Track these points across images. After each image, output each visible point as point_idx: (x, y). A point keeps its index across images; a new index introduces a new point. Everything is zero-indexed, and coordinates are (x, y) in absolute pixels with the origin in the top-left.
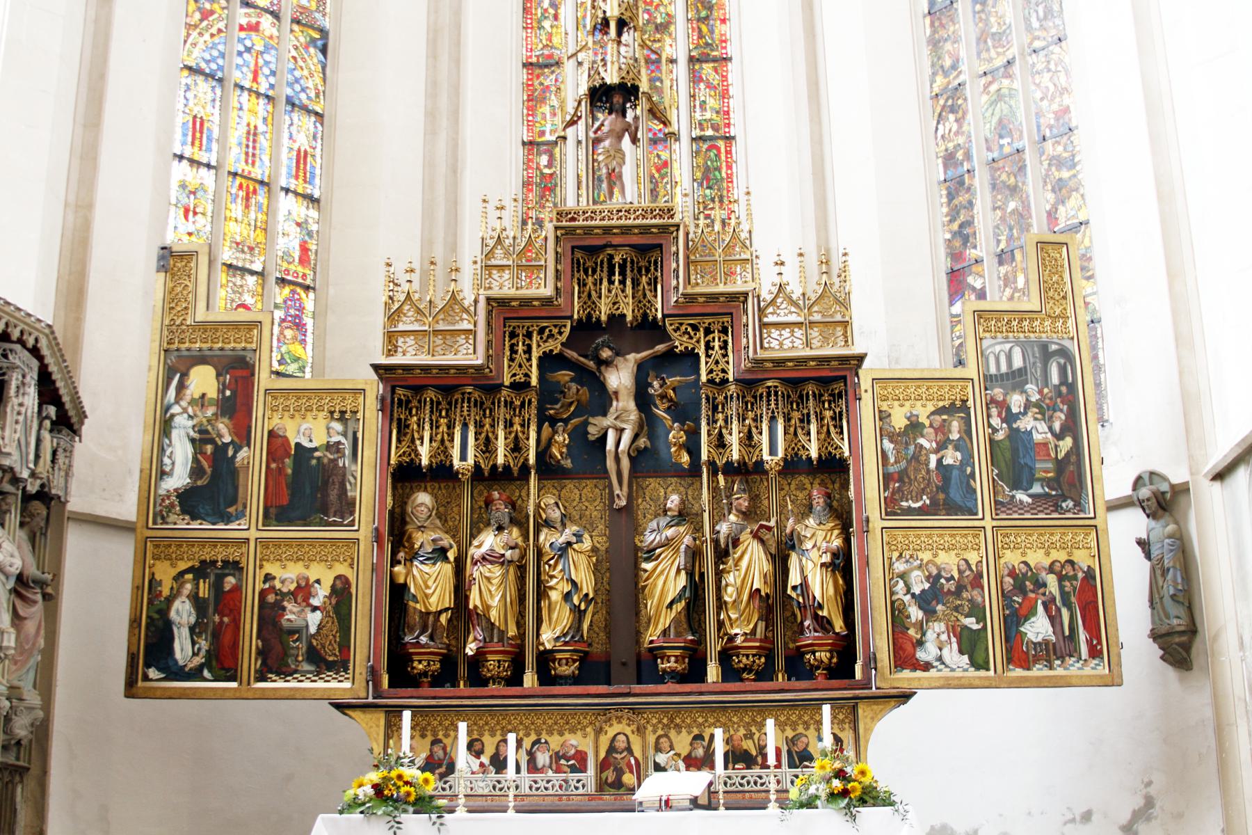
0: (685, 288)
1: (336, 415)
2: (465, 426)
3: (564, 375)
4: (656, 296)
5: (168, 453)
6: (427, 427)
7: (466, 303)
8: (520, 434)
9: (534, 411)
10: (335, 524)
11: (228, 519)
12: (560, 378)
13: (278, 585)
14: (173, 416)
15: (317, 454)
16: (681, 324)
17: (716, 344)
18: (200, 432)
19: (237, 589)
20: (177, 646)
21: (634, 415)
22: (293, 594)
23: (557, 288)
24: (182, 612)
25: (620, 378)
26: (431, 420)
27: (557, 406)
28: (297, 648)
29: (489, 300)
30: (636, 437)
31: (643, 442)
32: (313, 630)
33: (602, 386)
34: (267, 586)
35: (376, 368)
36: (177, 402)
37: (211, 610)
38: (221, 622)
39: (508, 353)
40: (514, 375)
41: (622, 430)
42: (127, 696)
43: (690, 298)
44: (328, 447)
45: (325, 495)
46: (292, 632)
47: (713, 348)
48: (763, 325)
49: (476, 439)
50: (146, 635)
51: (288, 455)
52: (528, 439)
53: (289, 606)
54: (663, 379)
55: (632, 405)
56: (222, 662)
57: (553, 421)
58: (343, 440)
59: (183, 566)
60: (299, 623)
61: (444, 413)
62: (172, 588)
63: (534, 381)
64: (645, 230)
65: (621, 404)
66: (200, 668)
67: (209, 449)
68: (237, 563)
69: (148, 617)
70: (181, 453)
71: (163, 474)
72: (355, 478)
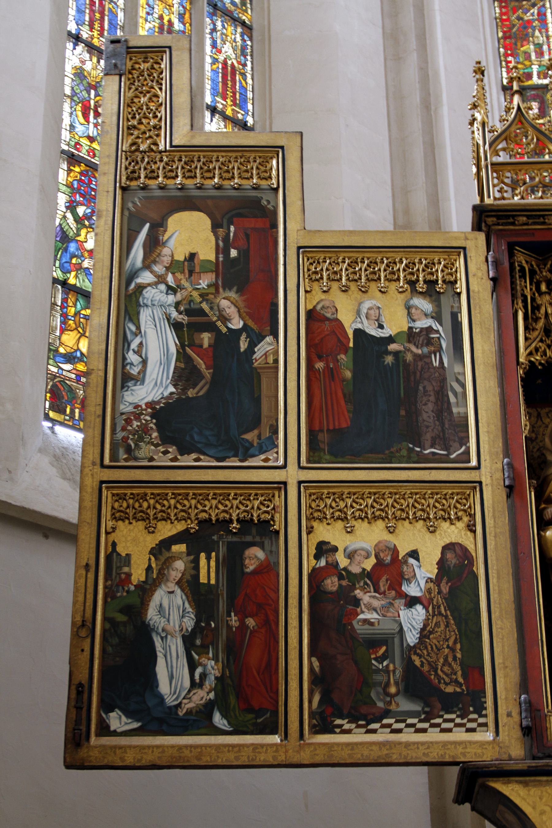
5: (134, 345)
10: (434, 458)
11: (245, 452)
13: (343, 562)
14: (141, 288)
15: (393, 347)
18: (189, 312)
19: (268, 569)
20: (161, 670)
22: (371, 577)
24: (169, 610)
28: (386, 670)
32: (412, 638)
34: (323, 563)
36: (147, 266)
37: (222, 605)
38: (243, 626)
42: (69, 766)
44: (411, 335)
45: (413, 413)
46: (373, 643)
50: (103, 651)
51: (346, 350)
53: (366, 597)
56: (247, 698)
58: (436, 326)
59: (167, 530)
60: (388, 627)
62: (149, 569)
66: (207, 710)
67: (206, 338)
68: (267, 522)
69: (105, 619)
70: (157, 345)
71: (126, 379)
72: (463, 386)
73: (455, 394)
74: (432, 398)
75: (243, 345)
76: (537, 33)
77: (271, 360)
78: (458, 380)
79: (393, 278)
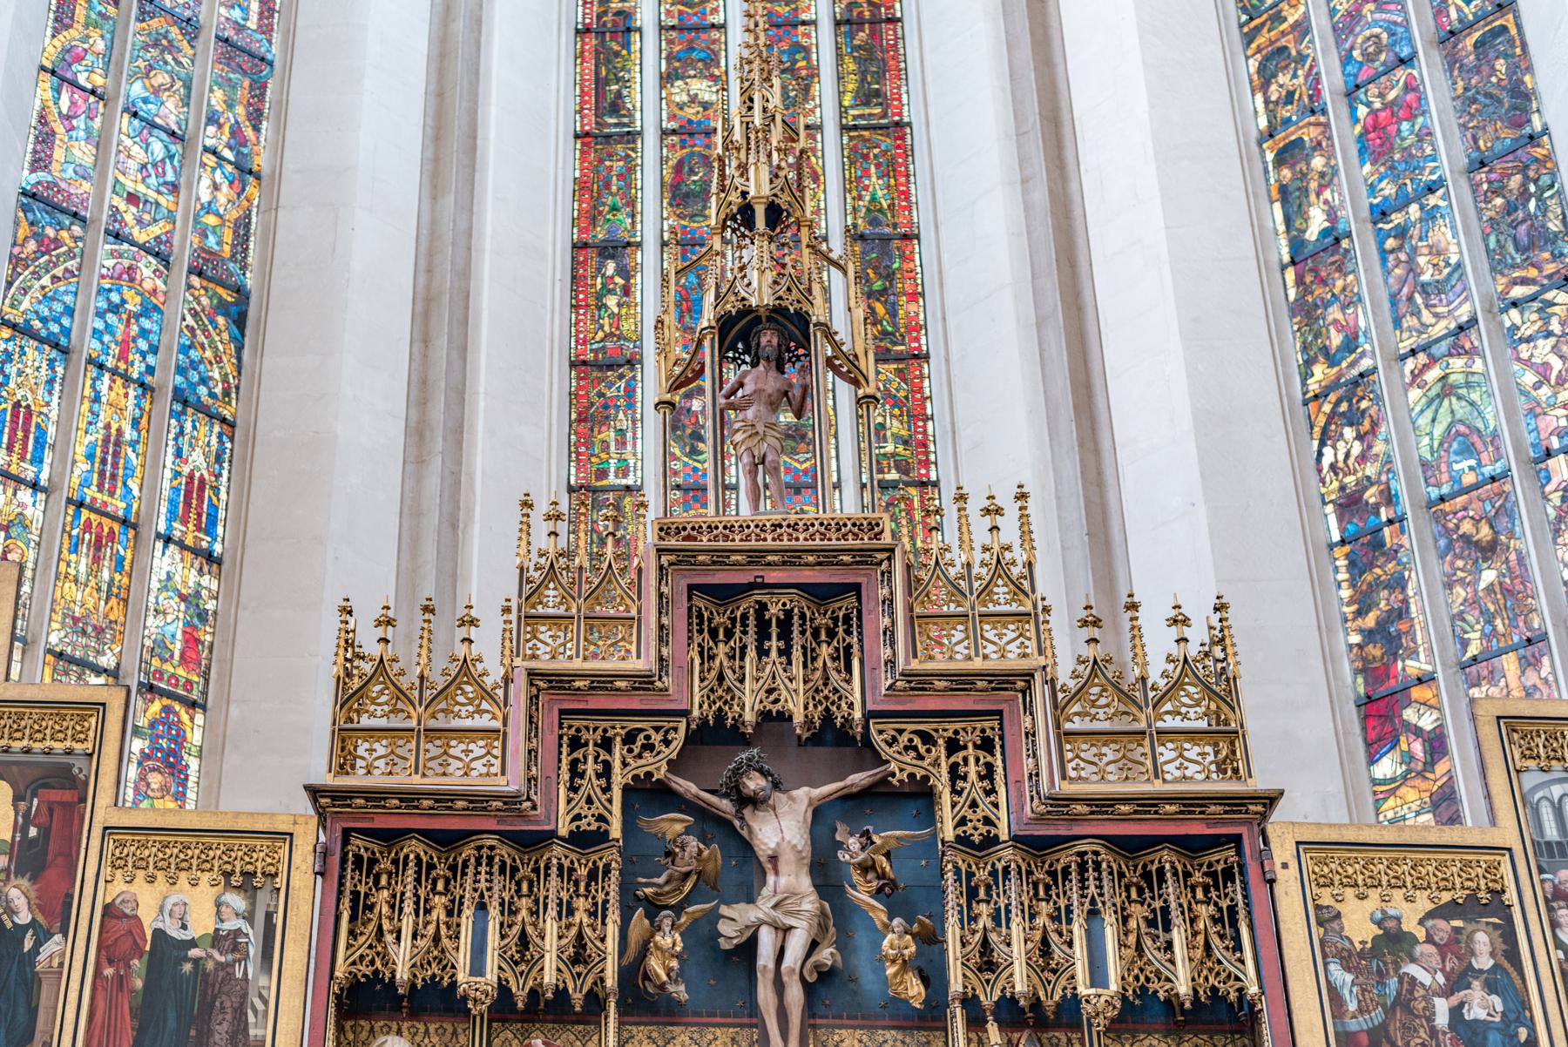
0: (907, 662)
1: (236, 880)
2: (482, 907)
3: (673, 824)
4: (848, 682)
6: (408, 907)
7: (489, 682)
8: (588, 931)
9: (613, 889)
12: (665, 826)
16: (901, 732)
17: (972, 770)
21: (810, 903)
23: (661, 659)
25: (781, 829)
26: (416, 895)
27: (661, 880)
29: (532, 674)
30: (814, 945)
31: (826, 955)
33: (746, 847)
35: (314, 792)
39: (566, 776)
40: (578, 817)
41: (788, 929)
43: (919, 682)
47: (964, 778)
48: (1064, 736)
49: (503, 937)
52: (603, 940)
54: (866, 834)
55: (805, 883)
57: (653, 908)
61: (440, 886)
63: (616, 831)
64: (828, 558)
65: (783, 881)
72: (266, 1002)
73: (255, 1012)
74: (228, 1017)
75: (28, 944)
76: (621, 416)
77: (55, 963)
78: (260, 996)
79: (205, 865)
